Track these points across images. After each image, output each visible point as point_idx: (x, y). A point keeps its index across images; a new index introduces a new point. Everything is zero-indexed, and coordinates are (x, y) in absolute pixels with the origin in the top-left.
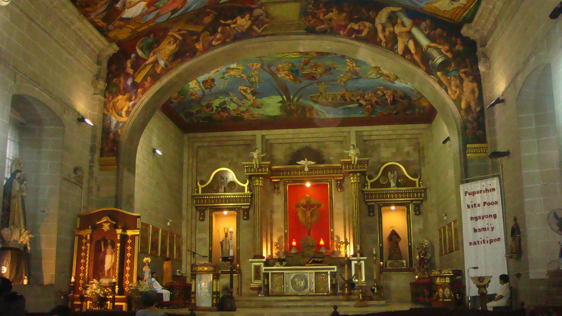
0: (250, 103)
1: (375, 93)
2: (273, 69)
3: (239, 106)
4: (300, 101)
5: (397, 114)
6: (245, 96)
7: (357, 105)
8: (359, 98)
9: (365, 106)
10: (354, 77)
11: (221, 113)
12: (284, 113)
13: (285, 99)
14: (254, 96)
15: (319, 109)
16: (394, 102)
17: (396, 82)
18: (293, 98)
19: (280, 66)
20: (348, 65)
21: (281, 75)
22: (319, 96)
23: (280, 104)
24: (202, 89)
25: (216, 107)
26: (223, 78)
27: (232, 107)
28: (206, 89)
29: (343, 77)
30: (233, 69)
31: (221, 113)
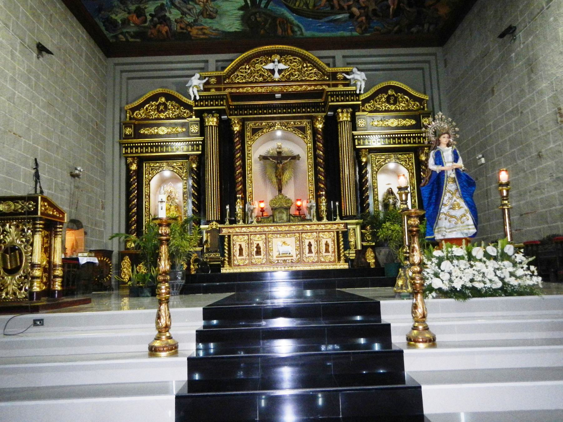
0: (198, 8)
3: (183, 13)
4: (269, 7)
5: (400, 31)
7: (347, 15)
8: (351, 3)
9: (360, 16)
11: (159, 25)
15: (296, 22)
16: (398, 11)
25: (151, 15)
27: (174, 14)
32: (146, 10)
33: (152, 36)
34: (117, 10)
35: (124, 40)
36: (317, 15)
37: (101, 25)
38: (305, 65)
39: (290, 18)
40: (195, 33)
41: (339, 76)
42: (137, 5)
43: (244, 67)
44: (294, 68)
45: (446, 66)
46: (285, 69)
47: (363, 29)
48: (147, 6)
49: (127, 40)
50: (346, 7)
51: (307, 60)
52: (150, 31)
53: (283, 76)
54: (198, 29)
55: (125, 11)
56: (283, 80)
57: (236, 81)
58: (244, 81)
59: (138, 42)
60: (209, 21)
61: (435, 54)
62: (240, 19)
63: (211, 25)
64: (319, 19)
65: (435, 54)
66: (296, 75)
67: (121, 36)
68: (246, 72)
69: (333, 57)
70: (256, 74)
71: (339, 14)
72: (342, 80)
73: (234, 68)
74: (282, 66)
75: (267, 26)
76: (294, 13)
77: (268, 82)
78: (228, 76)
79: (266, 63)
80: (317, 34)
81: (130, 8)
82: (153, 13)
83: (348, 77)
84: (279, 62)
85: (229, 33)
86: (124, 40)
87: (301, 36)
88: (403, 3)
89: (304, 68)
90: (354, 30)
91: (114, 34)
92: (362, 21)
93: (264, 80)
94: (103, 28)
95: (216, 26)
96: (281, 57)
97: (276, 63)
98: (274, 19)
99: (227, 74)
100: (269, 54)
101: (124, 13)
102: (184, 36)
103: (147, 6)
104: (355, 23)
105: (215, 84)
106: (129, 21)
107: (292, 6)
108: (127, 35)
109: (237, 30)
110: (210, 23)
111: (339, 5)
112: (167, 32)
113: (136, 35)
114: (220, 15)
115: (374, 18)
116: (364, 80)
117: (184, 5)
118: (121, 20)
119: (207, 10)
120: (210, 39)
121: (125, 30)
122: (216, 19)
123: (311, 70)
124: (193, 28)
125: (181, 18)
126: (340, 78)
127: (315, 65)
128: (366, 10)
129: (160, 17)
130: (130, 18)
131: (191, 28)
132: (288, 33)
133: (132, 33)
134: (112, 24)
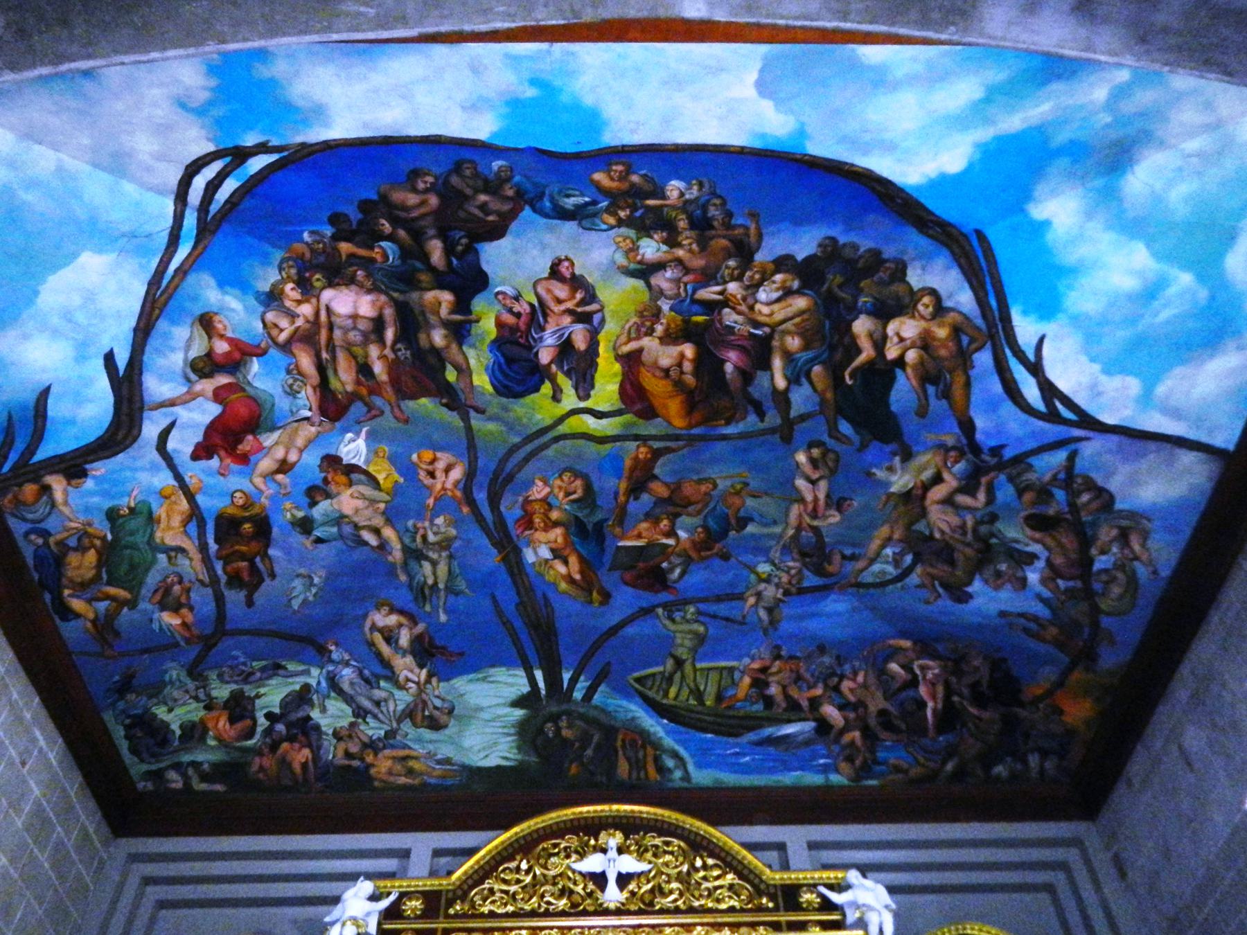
0: (403, 699)
1: (882, 672)
2: (511, 509)
3: (360, 713)
4: (597, 698)
6: (386, 664)
8: (819, 691)
10: (811, 580)
11: (285, 745)
12: (534, 759)
13: (541, 684)
14: (421, 667)
15: (668, 742)
16: (949, 718)
17: (977, 586)
18: (574, 681)
19: (538, 491)
20: (802, 500)
21: (538, 550)
22: (670, 680)
23: (519, 713)
24: (214, 581)
25: (269, 716)
26: (305, 525)
27: (331, 715)
28: (235, 580)
29: (768, 580)
30: (352, 469)
31: (285, 745)
32: (257, 701)
33: (261, 776)
34: (176, 694)
35: (179, 785)
36: (725, 722)
37: (119, 733)
38: (699, 863)
39: (652, 730)
40: (383, 770)
41: (807, 897)
42: (234, 687)
43: (513, 865)
44: (664, 870)
45: (1123, 874)
46: (639, 875)
47: (858, 763)
48: (262, 691)
49: (187, 784)
50: (805, 704)
51: (705, 849)
52: (257, 760)
53: (633, 894)
54: (394, 758)
55: (197, 699)
56: (633, 908)
57: (485, 910)
58: (510, 908)
59: (218, 792)
60: (427, 734)
61: (1076, 842)
62: (512, 731)
63: (431, 747)
64: (730, 735)
65: (1076, 842)
66: (671, 892)
67: (172, 775)
68: (518, 881)
69: (781, 847)
70: (548, 887)
71: (789, 721)
72: (815, 910)
73: (482, 867)
74: (629, 864)
75: (589, 752)
76: (663, 717)
77: (585, 913)
78: (462, 891)
79: (582, 855)
80: (730, 779)
81: (215, 693)
82: (277, 710)
83: (835, 897)
84: (620, 851)
85: (480, 769)
86: (179, 785)
87: (685, 785)
88: (960, 695)
89: (697, 870)
90: (837, 771)
91: (154, 767)
92: (852, 743)
93: (574, 905)
94: (123, 746)
95: (445, 751)
96: (627, 837)
97: (613, 853)
98: (610, 732)
99: (460, 887)
100: (593, 827)
101: (194, 705)
102: (353, 777)
103: (262, 691)
104: (835, 749)
105: (417, 917)
106: (205, 730)
107: (658, 698)
108: (190, 771)
109: (504, 763)
110: (431, 742)
111: (787, 697)
112: (304, 766)
113: (218, 772)
114: (459, 718)
115: (883, 735)
116: (887, 907)
117: (362, 688)
118: (181, 727)
119: (425, 703)
120: (425, 785)
121: (186, 758)
122: (447, 732)
123: (717, 878)
124: (380, 755)
125: (352, 725)
126: (808, 902)
127: (728, 862)
128: (861, 710)
129: (295, 722)
130: (210, 725)
131: (376, 755)
132: (646, 773)
133: (206, 766)
134: (150, 734)
